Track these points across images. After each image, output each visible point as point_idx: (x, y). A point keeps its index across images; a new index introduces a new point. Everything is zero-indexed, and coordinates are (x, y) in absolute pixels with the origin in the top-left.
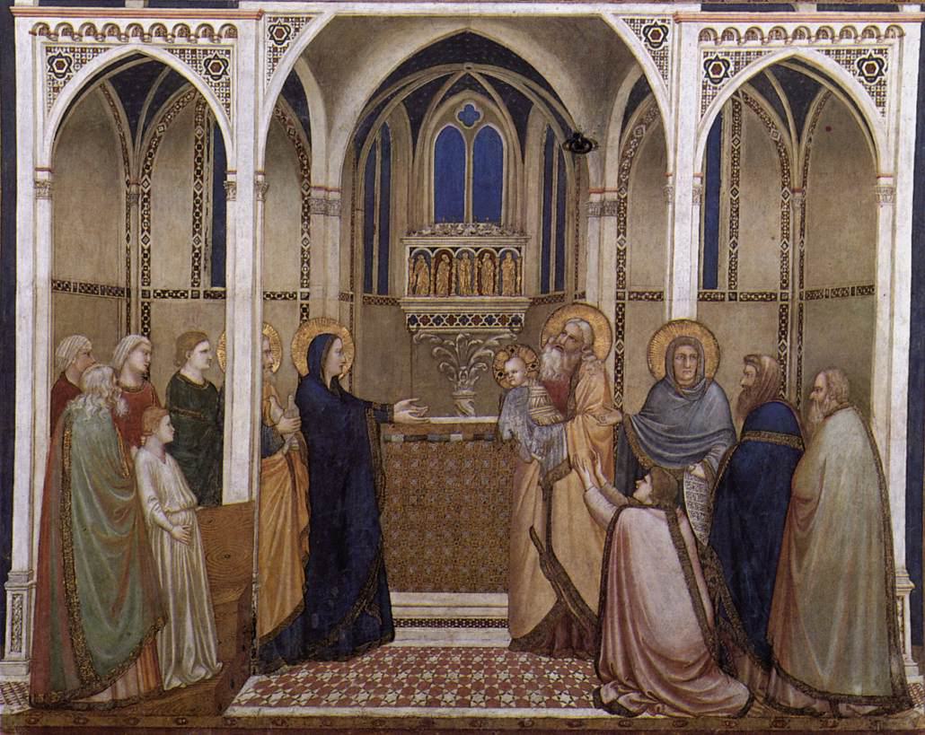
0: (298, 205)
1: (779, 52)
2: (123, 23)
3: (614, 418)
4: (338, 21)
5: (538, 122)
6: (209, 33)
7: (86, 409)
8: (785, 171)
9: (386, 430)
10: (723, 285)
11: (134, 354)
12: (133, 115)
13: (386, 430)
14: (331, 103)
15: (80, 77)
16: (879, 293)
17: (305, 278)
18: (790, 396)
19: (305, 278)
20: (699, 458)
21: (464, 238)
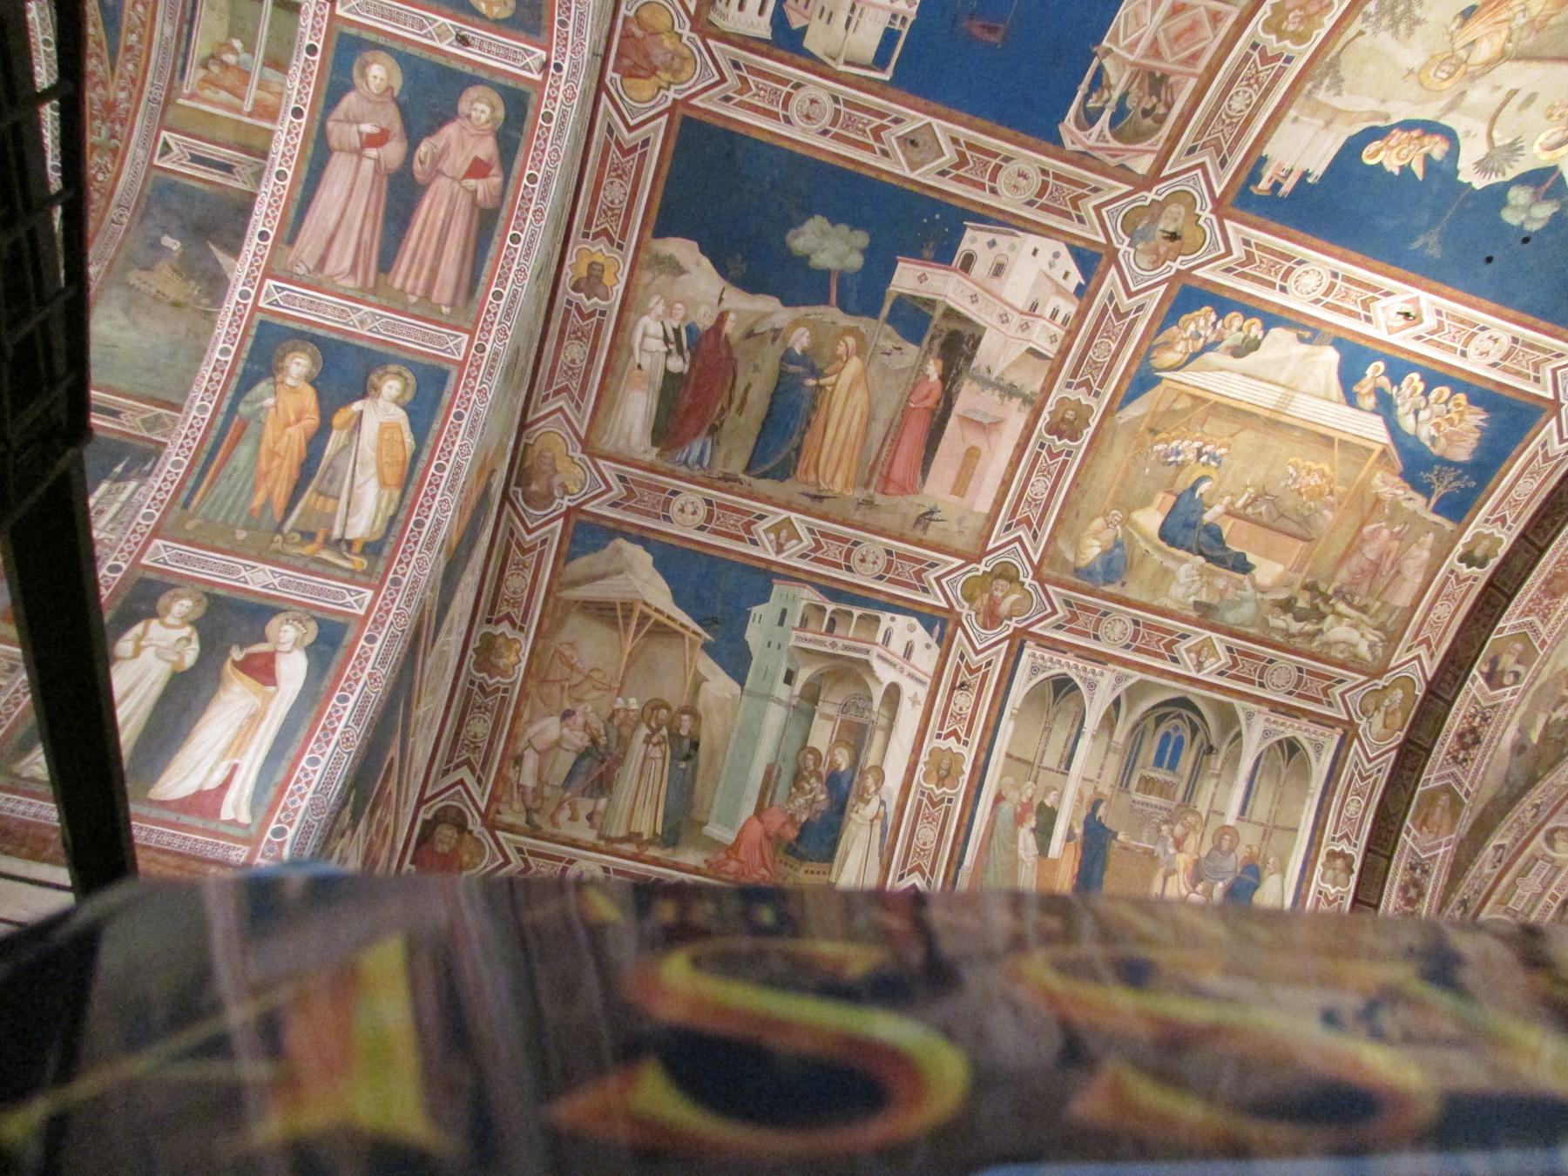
0: (1104, 748)
1: (1289, 733)
2: (1063, 661)
3: (1196, 857)
4: (1141, 683)
5: (1200, 736)
6: (1093, 672)
7: (1006, 807)
8: (1279, 777)
9: (1114, 842)
10: (1247, 817)
11: (1029, 790)
12: (1056, 696)
13: (1114, 842)
14: (1129, 710)
15: (1041, 677)
16: (1300, 832)
17: (1099, 776)
18: (1259, 863)
19: (1099, 776)
20: (1222, 880)
21: (1161, 775)
